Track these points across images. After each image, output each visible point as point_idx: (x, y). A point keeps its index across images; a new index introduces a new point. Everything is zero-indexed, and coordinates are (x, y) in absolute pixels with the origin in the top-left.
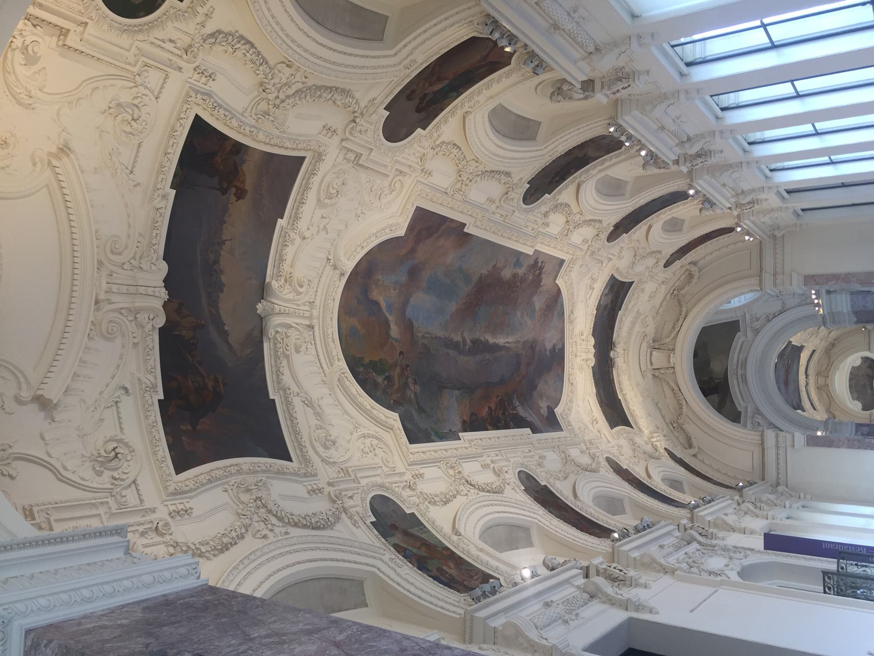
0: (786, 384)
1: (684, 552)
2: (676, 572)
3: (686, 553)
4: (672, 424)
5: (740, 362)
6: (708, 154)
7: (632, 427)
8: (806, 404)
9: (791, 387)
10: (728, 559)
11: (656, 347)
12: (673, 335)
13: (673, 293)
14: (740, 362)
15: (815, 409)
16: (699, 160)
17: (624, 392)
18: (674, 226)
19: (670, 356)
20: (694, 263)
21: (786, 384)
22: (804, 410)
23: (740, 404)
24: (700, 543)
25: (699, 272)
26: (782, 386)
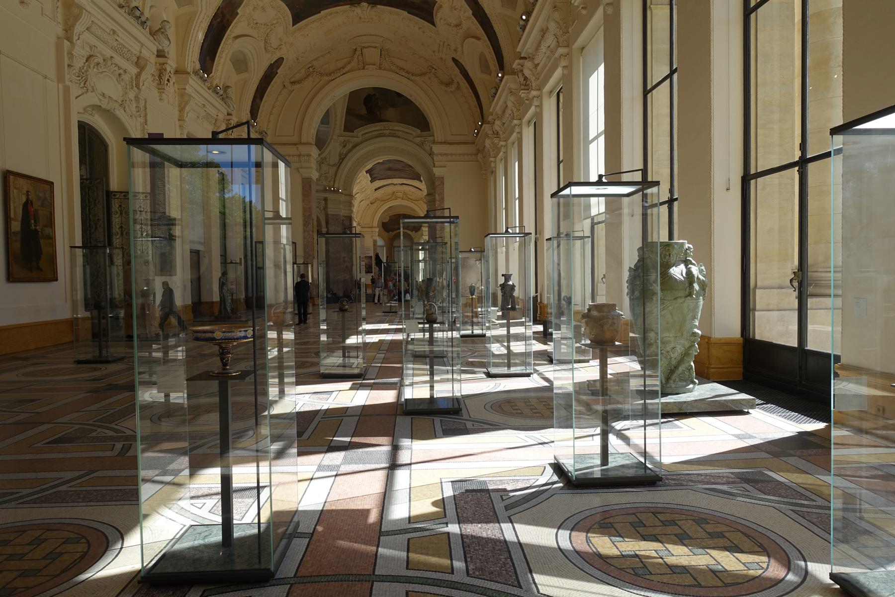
0: (390, 169)
1: (114, 55)
2: (66, 43)
3: (112, 57)
4: (311, 67)
5: (395, 132)
6: (526, 87)
7: (294, 25)
8: (378, 183)
9: (389, 173)
10: (121, 99)
11: (383, 52)
12: (394, 68)
13: (433, 68)
14: (395, 132)
15: (376, 190)
16: (522, 79)
17: (329, 17)
18: (484, 66)
19: (374, 65)
20: (458, 87)
21: (390, 169)
22: (371, 182)
23: (360, 132)
24: (138, 76)
25: (451, 91)
26: (387, 166)
